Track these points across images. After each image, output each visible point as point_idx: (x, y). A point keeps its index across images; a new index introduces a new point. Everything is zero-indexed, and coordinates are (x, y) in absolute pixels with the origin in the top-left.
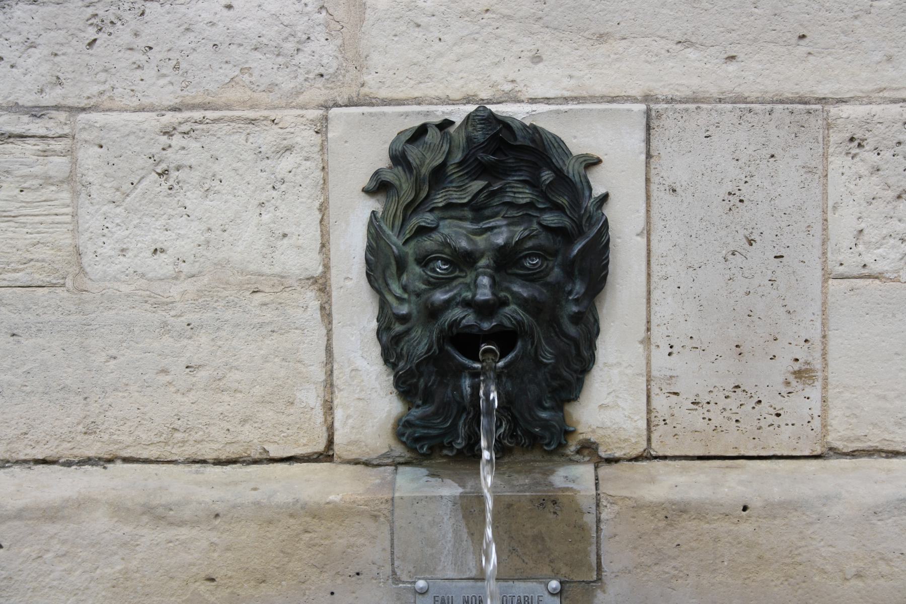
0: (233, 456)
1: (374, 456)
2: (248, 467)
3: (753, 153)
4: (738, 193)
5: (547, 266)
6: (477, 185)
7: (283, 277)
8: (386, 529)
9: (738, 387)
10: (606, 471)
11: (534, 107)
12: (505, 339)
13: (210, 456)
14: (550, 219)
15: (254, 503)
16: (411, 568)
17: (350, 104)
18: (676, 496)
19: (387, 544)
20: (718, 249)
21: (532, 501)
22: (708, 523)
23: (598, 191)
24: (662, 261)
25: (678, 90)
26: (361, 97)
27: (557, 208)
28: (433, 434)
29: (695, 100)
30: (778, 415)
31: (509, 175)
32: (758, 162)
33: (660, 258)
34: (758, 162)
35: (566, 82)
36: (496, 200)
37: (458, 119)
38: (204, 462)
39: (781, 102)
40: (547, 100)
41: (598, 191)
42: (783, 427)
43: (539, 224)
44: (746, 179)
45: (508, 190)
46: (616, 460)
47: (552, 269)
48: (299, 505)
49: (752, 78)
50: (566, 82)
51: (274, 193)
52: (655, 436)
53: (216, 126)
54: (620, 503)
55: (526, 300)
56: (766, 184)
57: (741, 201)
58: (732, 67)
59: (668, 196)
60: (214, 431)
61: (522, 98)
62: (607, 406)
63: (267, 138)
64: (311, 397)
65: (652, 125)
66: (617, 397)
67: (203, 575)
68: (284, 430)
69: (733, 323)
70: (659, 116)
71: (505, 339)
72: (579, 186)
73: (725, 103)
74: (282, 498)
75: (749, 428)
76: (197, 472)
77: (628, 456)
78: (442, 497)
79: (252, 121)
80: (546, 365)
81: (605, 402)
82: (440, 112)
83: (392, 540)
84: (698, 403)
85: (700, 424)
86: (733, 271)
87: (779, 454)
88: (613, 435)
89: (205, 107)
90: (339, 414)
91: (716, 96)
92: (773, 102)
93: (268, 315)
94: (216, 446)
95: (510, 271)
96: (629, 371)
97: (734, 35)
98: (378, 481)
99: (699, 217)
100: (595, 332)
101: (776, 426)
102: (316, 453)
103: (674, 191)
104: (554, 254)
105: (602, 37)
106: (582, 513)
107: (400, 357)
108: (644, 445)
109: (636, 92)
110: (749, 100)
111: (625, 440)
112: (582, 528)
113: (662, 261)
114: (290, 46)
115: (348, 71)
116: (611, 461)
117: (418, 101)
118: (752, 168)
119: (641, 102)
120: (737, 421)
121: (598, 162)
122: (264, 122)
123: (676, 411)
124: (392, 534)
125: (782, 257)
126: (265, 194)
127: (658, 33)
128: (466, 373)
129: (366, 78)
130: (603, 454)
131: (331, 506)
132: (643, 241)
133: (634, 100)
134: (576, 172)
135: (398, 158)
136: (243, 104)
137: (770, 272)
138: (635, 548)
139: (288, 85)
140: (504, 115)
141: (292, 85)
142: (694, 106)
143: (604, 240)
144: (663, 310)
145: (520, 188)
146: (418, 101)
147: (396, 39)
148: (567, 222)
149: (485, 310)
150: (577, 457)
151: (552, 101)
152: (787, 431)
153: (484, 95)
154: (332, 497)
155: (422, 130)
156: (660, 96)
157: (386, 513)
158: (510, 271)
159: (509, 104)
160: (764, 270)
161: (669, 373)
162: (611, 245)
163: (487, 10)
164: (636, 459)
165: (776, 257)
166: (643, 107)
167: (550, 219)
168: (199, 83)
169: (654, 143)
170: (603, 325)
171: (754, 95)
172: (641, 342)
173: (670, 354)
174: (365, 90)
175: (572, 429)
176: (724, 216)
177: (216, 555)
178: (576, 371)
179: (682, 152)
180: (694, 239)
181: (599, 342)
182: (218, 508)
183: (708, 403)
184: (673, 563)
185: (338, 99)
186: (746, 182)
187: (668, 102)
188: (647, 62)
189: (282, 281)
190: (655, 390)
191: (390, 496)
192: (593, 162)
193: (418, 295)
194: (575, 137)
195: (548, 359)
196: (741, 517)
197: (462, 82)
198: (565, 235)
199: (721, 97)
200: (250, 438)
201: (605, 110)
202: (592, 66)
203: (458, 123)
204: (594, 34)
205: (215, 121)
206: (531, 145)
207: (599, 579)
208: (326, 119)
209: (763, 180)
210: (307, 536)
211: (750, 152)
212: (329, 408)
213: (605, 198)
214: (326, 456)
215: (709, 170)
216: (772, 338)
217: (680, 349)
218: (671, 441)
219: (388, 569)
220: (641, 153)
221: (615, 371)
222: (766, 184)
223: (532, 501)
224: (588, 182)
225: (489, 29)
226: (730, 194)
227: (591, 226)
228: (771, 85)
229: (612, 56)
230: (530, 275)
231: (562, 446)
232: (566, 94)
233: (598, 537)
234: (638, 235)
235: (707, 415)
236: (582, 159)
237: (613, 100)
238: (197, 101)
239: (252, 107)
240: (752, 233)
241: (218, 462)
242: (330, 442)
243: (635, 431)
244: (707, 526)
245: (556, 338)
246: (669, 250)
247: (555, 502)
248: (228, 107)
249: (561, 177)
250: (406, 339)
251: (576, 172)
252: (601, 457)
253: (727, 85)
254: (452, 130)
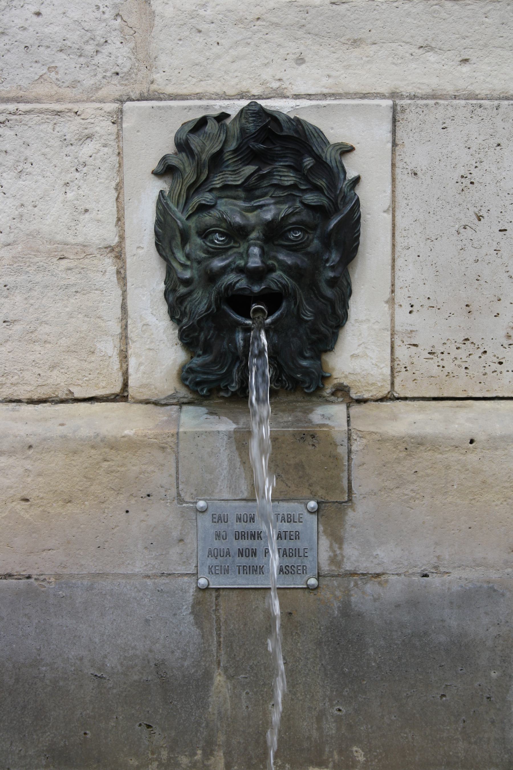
0: (44, 397)
1: (162, 397)
2: (56, 405)
3: (483, 143)
4: (469, 176)
5: (308, 238)
6: (249, 169)
7: (85, 246)
8: (172, 459)
9: (467, 339)
10: (356, 409)
11: (298, 102)
12: (272, 300)
13: (24, 396)
14: (311, 198)
15: (61, 437)
16: (193, 491)
17: (142, 98)
18: (415, 431)
19: (173, 471)
20: (452, 224)
21: (294, 435)
22: (441, 453)
23: (351, 174)
24: (405, 233)
25: (419, 88)
26: (151, 93)
27: (317, 189)
28: (212, 380)
29: (434, 97)
30: (501, 363)
31: (276, 161)
32: (486, 150)
33: (403, 231)
34: (486, 150)
35: (325, 81)
36: (265, 182)
37: (233, 113)
38: (19, 401)
39: (507, 99)
40: (309, 96)
41: (351, 174)
42: (505, 373)
43: (302, 202)
44: (476, 165)
45: (275, 173)
46: (365, 401)
47: (312, 241)
48: (99, 439)
49: (482, 78)
50: (325, 81)
51: (77, 175)
52: (397, 381)
53: (27, 117)
54: (368, 437)
55: (290, 267)
56: (493, 168)
57: (472, 183)
58: (465, 69)
59: (410, 179)
60: (27, 375)
61: (288, 94)
63: (71, 127)
64: (109, 348)
65: (397, 118)
66: (366, 348)
67: (19, 496)
68: (87, 375)
69: (464, 286)
70: (403, 111)
71: (272, 300)
72: (335, 170)
73: (459, 99)
74: (85, 432)
75: (476, 374)
76: (13, 410)
77: (374, 398)
78: (219, 432)
79: (58, 113)
80: (307, 321)
81: (356, 352)
82: (218, 106)
83: (177, 467)
84: (434, 353)
85: (435, 371)
86: (465, 242)
87: (501, 395)
88: (362, 380)
89: (18, 100)
90: (132, 362)
91: (451, 93)
92: (499, 99)
93: (73, 278)
94: (29, 388)
95: (276, 243)
96: (376, 327)
97: (468, 41)
98: (165, 418)
99: (436, 197)
100: (348, 294)
101: (498, 372)
102: (113, 394)
103: (415, 174)
104: (314, 228)
105: (356, 43)
106: (336, 445)
107: (184, 314)
108: (389, 388)
109: (384, 90)
110: (479, 97)
111: (373, 384)
112: (336, 458)
113: (405, 233)
114: (90, 48)
115: (139, 70)
116: (360, 401)
117: (199, 97)
118: (482, 155)
119: (388, 98)
120: (466, 368)
121: (352, 149)
122: (69, 114)
123: (415, 360)
124: (177, 462)
125: (506, 230)
126: (70, 175)
127: (403, 39)
128: (239, 329)
129: (155, 76)
130: (354, 396)
131: (126, 439)
132: (389, 217)
133: (382, 96)
134: (333, 158)
135: (182, 146)
136: (51, 98)
137: (495, 243)
138: (380, 474)
139: (88, 82)
140: (272, 109)
141: (92, 82)
142: (431, 102)
143: (356, 216)
144: (404, 276)
145: (285, 172)
146: (199, 97)
147: (181, 43)
148: (325, 201)
149: (256, 275)
150: (332, 398)
151: (312, 97)
152: (507, 377)
153: (255, 91)
154: (126, 432)
155: (203, 122)
156: (404, 93)
157: (172, 445)
158: (276, 243)
159: (276, 100)
160: (491, 241)
161: (409, 328)
162: (362, 220)
163: (258, 19)
164: (382, 400)
165: (500, 231)
166: (390, 102)
167: (311, 198)
168: (12, 80)
169: (399, 134)
170: (355, 288)
171: (485, 92)
172: (387, 302)
173: (411, 312)
174: (154, 87)
175: (328, 375)
176: (458, 196)
177: (29, 480)
178: (331, 327)
179: (423, 142)
180: (432, 215)
181: (352, 302)
182: (31, 440)
183: (442, 353)
184: (412, 487)
185: (132, 94)
186: (476, 167)
187: (411, 99)
188: (394, 63)
189: (84, 249)
190: (398, 342)
191: (175, 431)
192: (347, 150)
193: (199, 262)
194: (332, 128)
195: (308, 317)
196: (469, 449)
197: (237, 80)
198: (323, 212)
199: (456, 94)
200: (58, 382)
201: (357, 105)
202: (347, 67)
203: (233, 116)
204: (349, 40)
205: (27, 112)
206: (295, 135)
207: (350, 500)
208: (121, 111)
209: (491, 165)
210: (105, 464)
211: (480, 141)
212: (124, 357)
213: (357, 180)
214: (122, 396)
215: (445, 157)
216: (496, 299)
217: (419, 308)
218: (412, 384)
219: (173, 492)
220: (388, 142)
221: (365, 326)
222: (493, 168)
223: (294, 435)
224: (343, 167)
225: (260, 35)
226: (462, 177)
227: (345, 204)
228: (499, 84)
229: (364, 58)
230: (293, 246)
231: (320, 388)
232: (325, 91)
233: (349, 465)
234: (385, 212)
235: (441, 363)
236: (338, 147)
237: (364, 96)
238: (11, 95)
239: (58, 101)
240: (480, 210)
241: (31, 402)
242: (125, 385)
243: (381, 377)
244: (440, 456)
245: (315, 299)
246: (411, 224)
247: (313, 436)
248: (38, 100)
249: (320, 161)
250: (189, 299)
251: (333, 158)
252: (352, 398)
253: (461, 84)
254: (228, 121)
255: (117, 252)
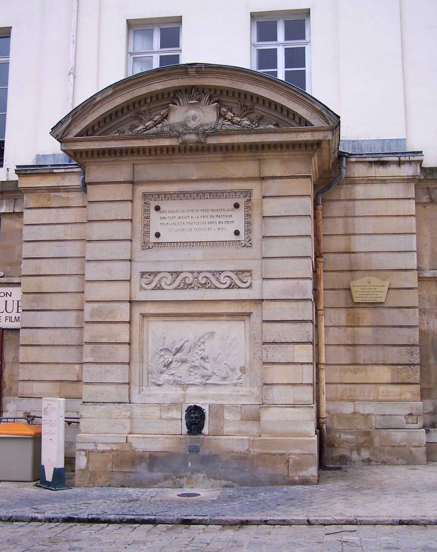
12: (195, 424)
28: (190, 433)
62: (205, 430)
63: (177, 407)
149: (194, 421)
157: (186, 438)
200: (174, 433)
214: (181, 434)
255: (181, 420)
